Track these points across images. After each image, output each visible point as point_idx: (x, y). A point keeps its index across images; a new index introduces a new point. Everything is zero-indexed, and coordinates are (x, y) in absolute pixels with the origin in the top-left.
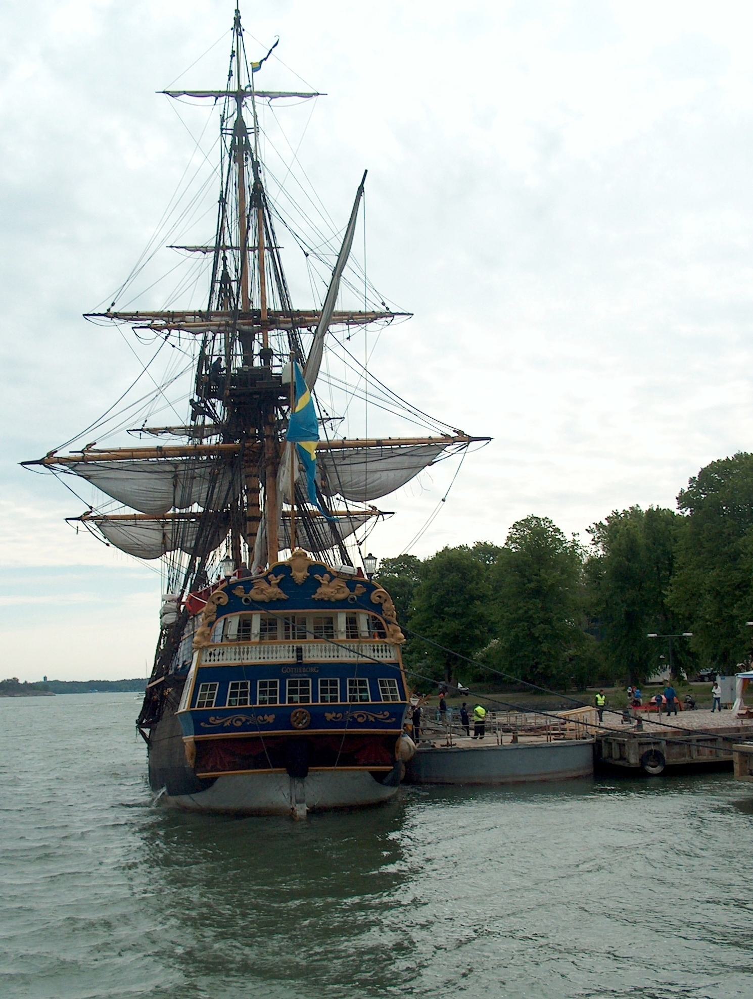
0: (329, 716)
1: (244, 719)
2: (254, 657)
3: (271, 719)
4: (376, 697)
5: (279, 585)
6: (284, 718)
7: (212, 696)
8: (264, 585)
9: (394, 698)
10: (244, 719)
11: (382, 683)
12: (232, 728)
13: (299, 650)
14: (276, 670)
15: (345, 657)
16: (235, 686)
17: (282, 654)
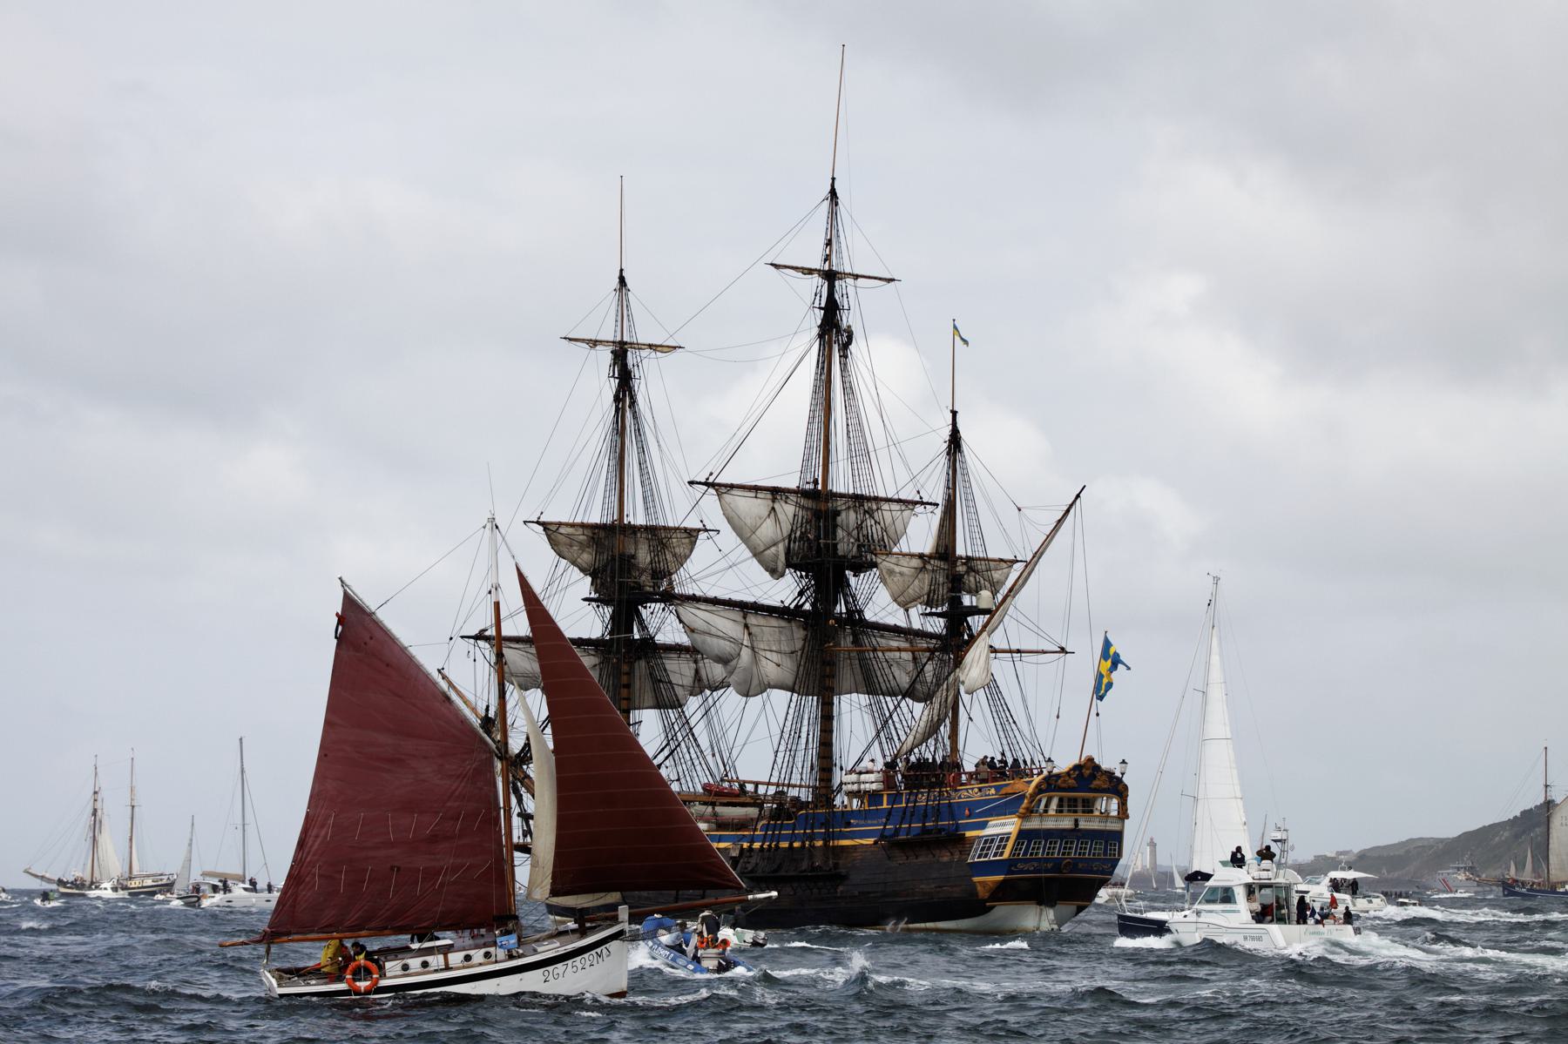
7: (1021, 849)
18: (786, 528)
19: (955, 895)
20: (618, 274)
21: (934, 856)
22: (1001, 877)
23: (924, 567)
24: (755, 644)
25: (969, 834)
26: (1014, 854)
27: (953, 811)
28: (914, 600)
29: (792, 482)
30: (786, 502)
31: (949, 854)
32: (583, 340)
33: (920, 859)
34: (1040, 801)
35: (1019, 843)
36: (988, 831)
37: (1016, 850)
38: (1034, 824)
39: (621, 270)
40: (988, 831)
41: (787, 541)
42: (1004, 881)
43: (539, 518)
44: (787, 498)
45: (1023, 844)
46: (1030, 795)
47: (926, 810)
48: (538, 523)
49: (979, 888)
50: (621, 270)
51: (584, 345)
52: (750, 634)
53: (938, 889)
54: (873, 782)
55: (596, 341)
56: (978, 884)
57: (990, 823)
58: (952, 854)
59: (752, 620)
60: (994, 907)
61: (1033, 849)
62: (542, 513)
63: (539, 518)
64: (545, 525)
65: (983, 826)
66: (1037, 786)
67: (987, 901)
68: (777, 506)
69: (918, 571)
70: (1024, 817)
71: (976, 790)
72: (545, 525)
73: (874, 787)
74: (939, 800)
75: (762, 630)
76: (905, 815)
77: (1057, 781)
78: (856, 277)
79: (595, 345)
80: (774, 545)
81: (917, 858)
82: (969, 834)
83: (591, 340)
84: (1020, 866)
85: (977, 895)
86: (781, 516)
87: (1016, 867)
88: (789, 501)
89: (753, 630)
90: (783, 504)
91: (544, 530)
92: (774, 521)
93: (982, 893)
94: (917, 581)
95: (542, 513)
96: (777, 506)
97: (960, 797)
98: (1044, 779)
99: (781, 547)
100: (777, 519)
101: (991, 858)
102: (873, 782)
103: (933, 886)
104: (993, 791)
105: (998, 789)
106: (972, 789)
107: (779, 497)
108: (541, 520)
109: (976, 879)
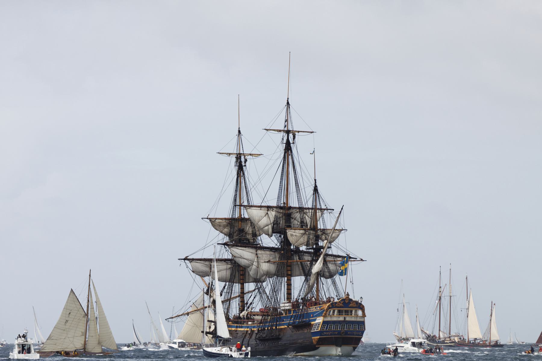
0: (349, 333)
1: (331, 333)
2: (335, 319)
3: (336, 333)
4: (359, 329)
5: (342, 303)
6: (339, 333)
7: (325, 327)
8: (339, 303)
9: (362, 329)
10: (331, 333)
11: (360, 326)
12: (328, 335)
13: (345, 318)
14: (340, 322)
15: (353, 319)
16: (330, 325)
17: (341, 319)
18: (272, 220)
19: (308, 343)
20: (238, 130)
21: (303, 331)
22: (318, 337)
23: (305, 233)
24: (259, 261)
25: (312, 323)
26: (322, 329)
27: (308, 315)
28: (301, 244)
29: (274, 203)
30: (273, 211)
31: (307, 330)
32: (225, 153)
33: (300, 332)
34: (330, 311)
35: (323, 326)
36: (316, 322)
37: (323, 328)
38: (328, 319)
39: (239, 128)
40: (316, 322)
41: (272, 224)
42: (320, 338)
43: (208, 217)
44: (273, 209)
45: (325, 326)
46: (326, 309)
47: (300, 315)
48: (207, 218)
49: (313, 341)
50: (239, 128)
51: (226, 155)
52: (257, 257)
53: (303, 342)
54: (288, 306)
55: (230, 154)
56: (313, 340)
57: (317, 319)
58: (308, 330)
59: (259, 252)
60: (319, 347)
61: (329, 327)
62: (209, 215)
63: (208, 217)
64: (210, 219)
65: (315, 320)
66: (328, 306)
67: (316, 345)
68: (269, 212)
69: (303, 234)
70: (324, 317)
71: (315, 308)
72: (210, 219)
73: (288, 308)
74: (304, 312)
75: (262, 255)
76: (296, 317)
77: (335, 305)
78: (299, 132)
79: (230, 155)
80: (267, 226)
81: (299, 331)
82: (312, 323)
83: (228, 153)
84: (325, 333)
85: (313, 343)
86: (270, 216)
87: (323, 334)
88: (273, 211)
89: (259, 256)
90: (271, 212)
91: (210, 221)
92: (267, 218)
93: (314, 342)
94: (302, 238)
95: (209, 215)
96: (269, 212)
97: (310, 311)
98: (331, 304)
99: (270, 227)
100: (269, 217)
101: (316, 331)
102: (288, 306)
103: (302, 341)
104: (319, 308)
105: (320, 307)
106: (314, 308)
107: (270, 209)
108: (209, 217)
109: (313, 338)
